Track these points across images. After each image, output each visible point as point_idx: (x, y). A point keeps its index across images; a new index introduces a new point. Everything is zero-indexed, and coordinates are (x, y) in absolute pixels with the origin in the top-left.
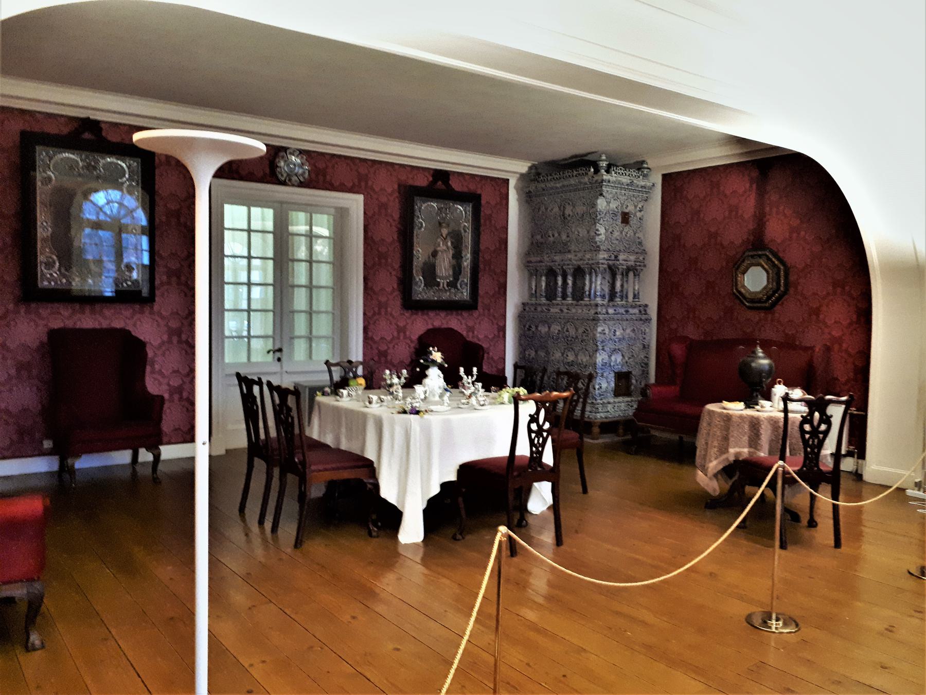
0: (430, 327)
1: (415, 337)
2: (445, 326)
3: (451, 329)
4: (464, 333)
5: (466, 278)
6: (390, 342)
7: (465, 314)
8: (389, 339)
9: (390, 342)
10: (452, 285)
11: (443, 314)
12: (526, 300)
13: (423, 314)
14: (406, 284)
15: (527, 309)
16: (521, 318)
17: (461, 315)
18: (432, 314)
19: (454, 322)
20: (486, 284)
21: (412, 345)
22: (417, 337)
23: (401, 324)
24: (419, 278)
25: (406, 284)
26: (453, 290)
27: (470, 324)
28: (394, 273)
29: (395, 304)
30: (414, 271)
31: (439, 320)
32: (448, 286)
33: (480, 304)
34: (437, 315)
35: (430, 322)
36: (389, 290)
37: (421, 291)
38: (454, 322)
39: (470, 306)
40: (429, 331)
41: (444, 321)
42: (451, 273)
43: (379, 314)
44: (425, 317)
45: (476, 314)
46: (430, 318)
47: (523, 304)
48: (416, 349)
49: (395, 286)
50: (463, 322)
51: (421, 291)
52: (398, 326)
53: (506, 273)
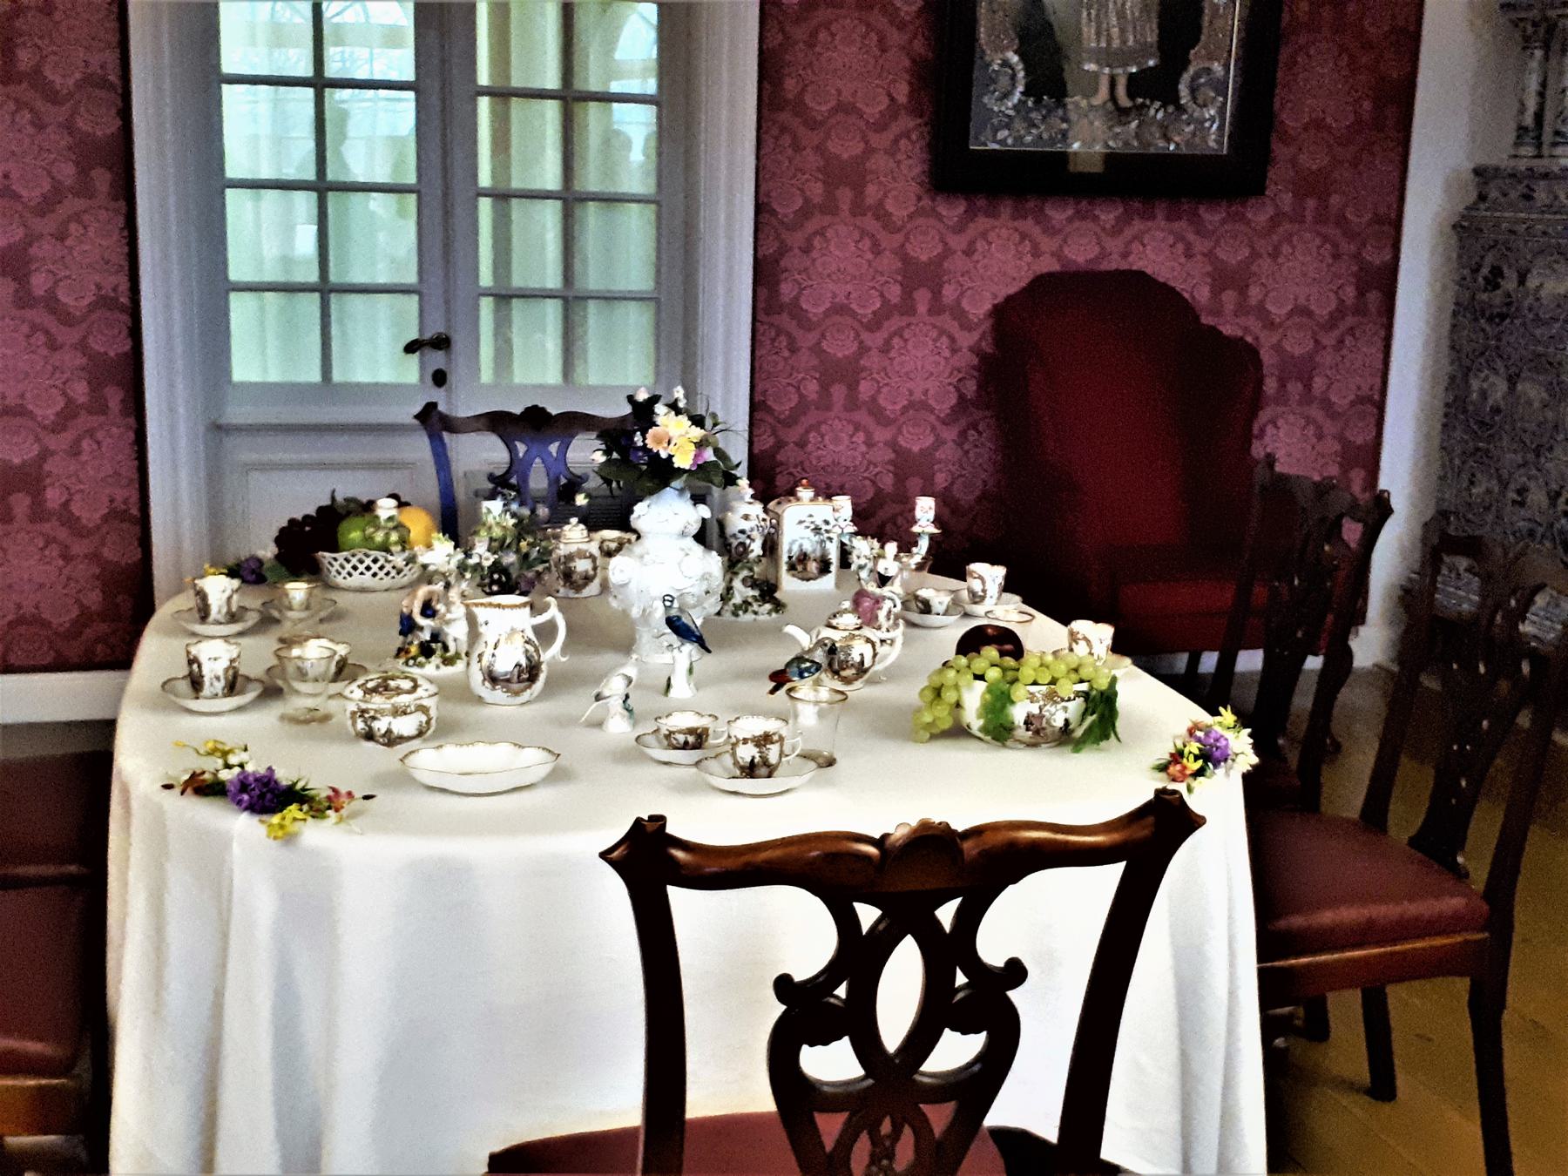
0: (1048, 265)
1: (979, 307)
2: (1114, 264)
3: (1141, 274)
4: (1202, 295)
5: (1217, 61)
6: (875, 324)
7: (1212, 217)
8: (867, 312)
9: (875, 324)
10: (1156, 85)
11: (1108, 215)
12: (1500, 154)
13: (1019, 215)
14: (946, 83)
15: (1494, 194)
16: (1466, 231)
17: (1195, 219)
18: (1058, 214)
19: (1158, 250)
20: (1316, 90)
21: (967, 339)
22: (988, 306)
23: (924, 250)
24: (1003, 58)
25: (946, 83)
26: (1157, 112)
27: (1233, 254)
28: (895, 37)
29: (899, 172)
30: (982, 33)
31: (1084, 241)
32: (1131, 95)
33: (1278, 180)
34: (1080, 215)
35: (1048, 244)
36: (875, 109)
37: (1003, 117)
38: (1158, 250)
39: (1228, 180)
40: (1040, 283)
41: (1114, 245)
42: (1152, 37)
43: (830, 208)
44: (1028, 225)
45: (1259, 215)
46: (1051, 231)
47: (1478, 172)
48: (983, 357)
49: (902, 92)
50: (1200, 245)
51: (1003, 117)
52: (906, 259)
53: (1415, 38)
